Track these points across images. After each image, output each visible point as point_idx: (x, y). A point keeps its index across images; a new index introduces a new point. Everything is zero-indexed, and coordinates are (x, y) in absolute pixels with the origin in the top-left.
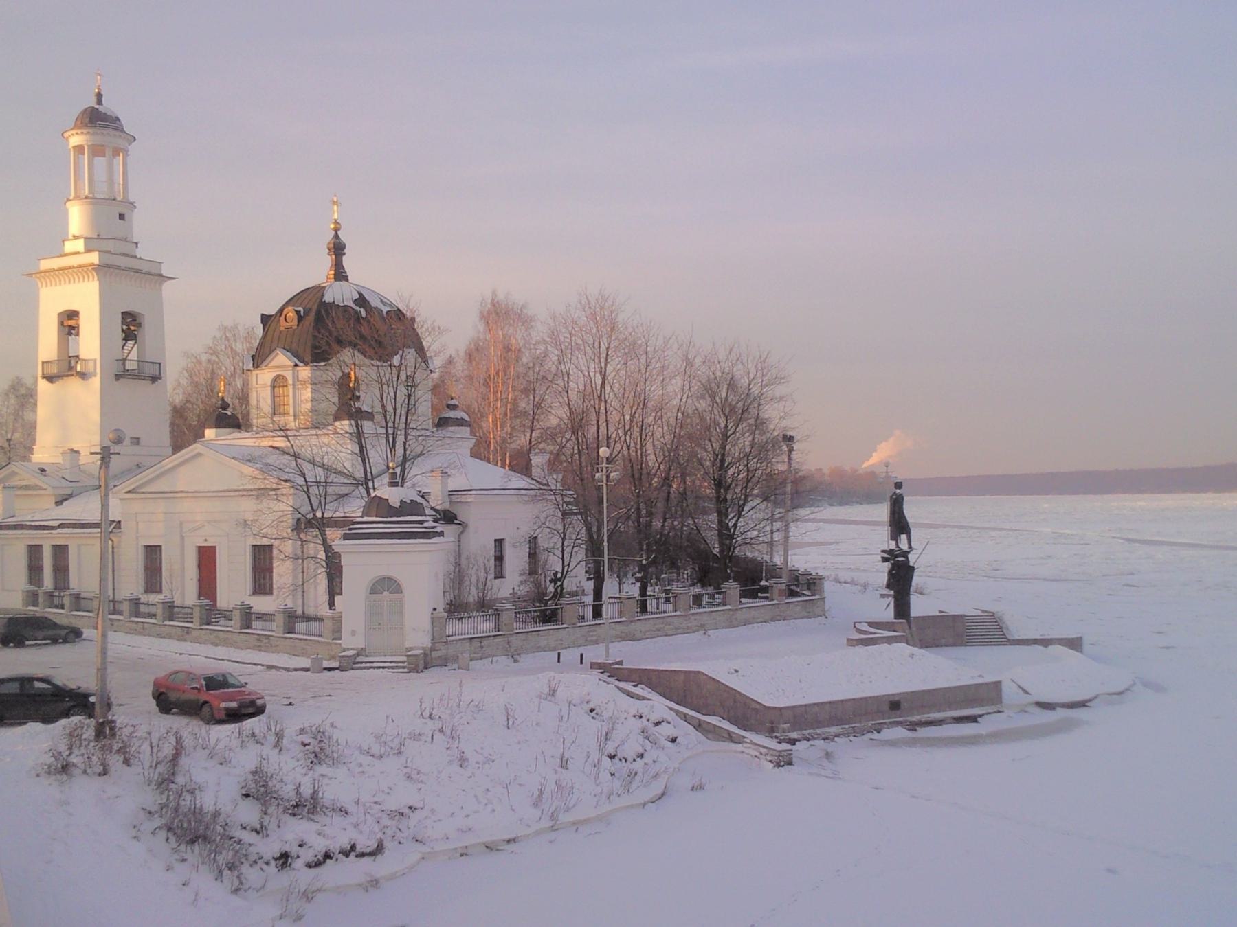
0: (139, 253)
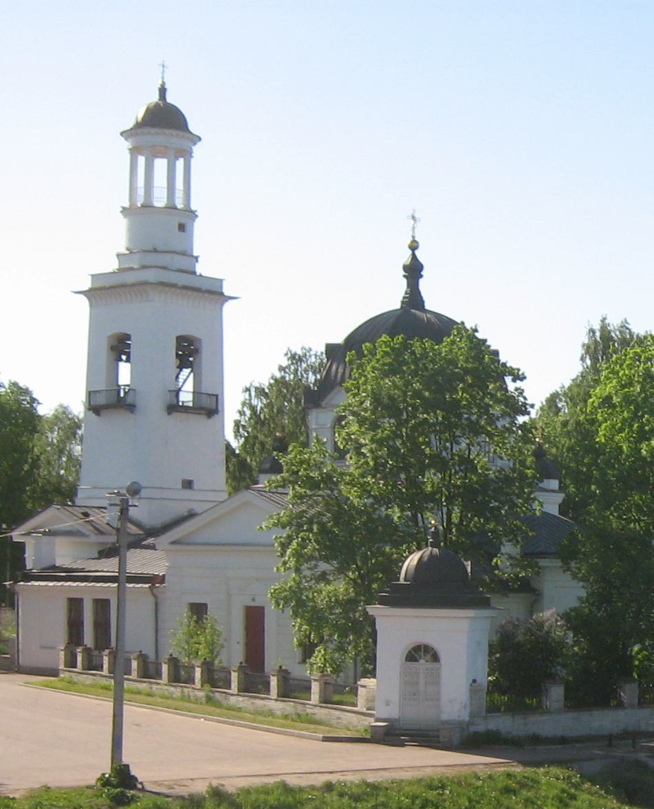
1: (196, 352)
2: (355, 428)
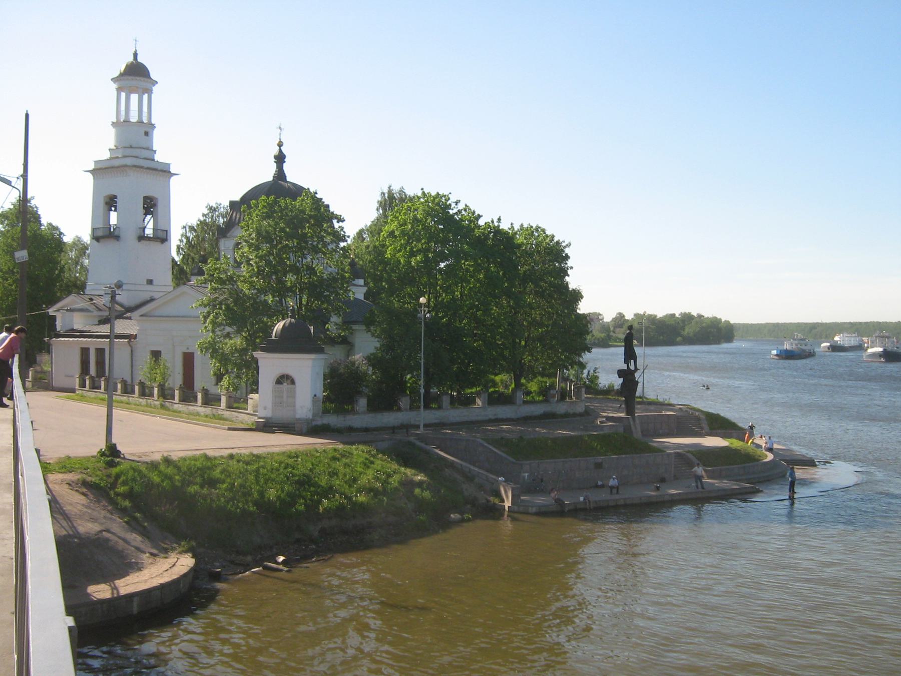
0: (156, 159)
1: (155, 206)
2: (246, 249)
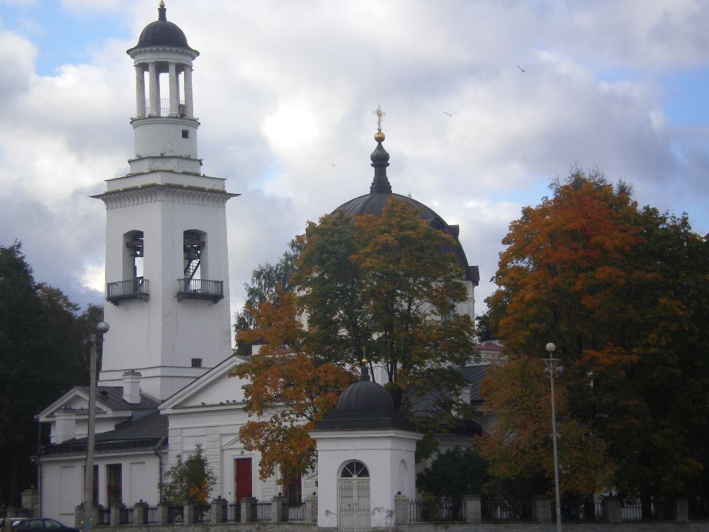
1: (202, 245)
